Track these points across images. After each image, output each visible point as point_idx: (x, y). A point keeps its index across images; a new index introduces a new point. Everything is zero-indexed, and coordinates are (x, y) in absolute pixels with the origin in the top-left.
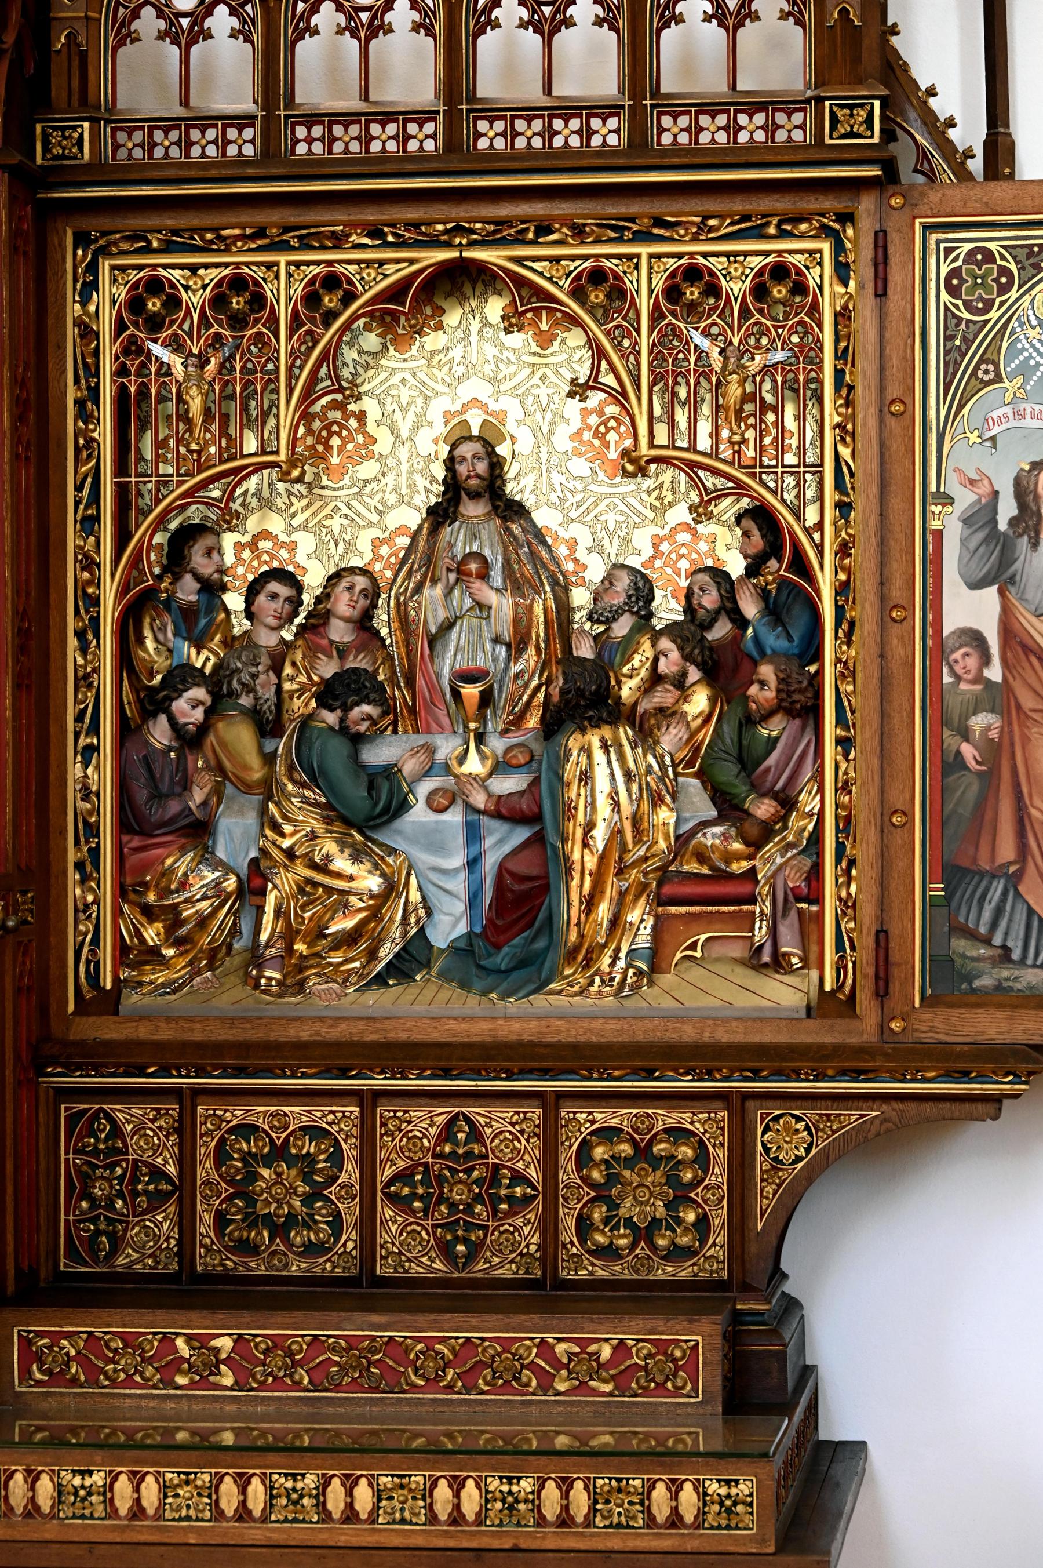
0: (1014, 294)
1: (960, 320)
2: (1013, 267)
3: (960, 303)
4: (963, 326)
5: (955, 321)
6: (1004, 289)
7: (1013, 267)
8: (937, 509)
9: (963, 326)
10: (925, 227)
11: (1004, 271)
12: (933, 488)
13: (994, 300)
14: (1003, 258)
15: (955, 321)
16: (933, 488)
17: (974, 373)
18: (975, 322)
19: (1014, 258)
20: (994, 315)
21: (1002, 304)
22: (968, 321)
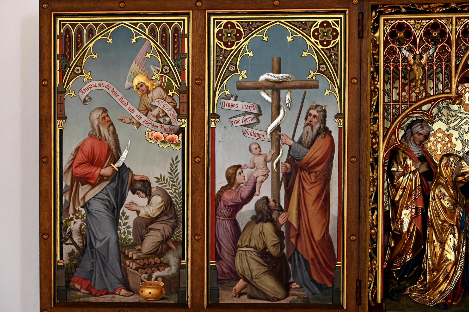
0: (242, 40)
1: (222, 49)
2: (242, 30)
3: (222, 43)
4: (223, 52)
5: (220, 50)
6: (238, 39)
7: (242, 30)
8: (213, 120)
9: (223, 52)
10: (210, 14)
11: (239, 31)
12: (211, 112)
13: (235, 42)
14: (238, 26)
15: (220, 50)
16: (211, 112)
17: (228, 68)
18: (227, 50)
19: (242, 26)
20: (234, 47)
21: (237, 44)
22: (225, 50)
